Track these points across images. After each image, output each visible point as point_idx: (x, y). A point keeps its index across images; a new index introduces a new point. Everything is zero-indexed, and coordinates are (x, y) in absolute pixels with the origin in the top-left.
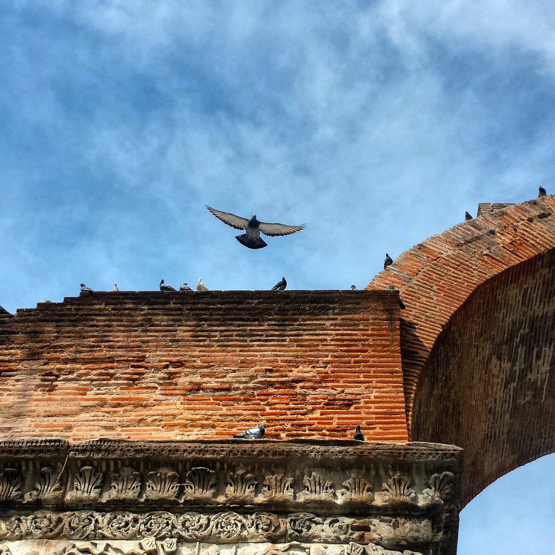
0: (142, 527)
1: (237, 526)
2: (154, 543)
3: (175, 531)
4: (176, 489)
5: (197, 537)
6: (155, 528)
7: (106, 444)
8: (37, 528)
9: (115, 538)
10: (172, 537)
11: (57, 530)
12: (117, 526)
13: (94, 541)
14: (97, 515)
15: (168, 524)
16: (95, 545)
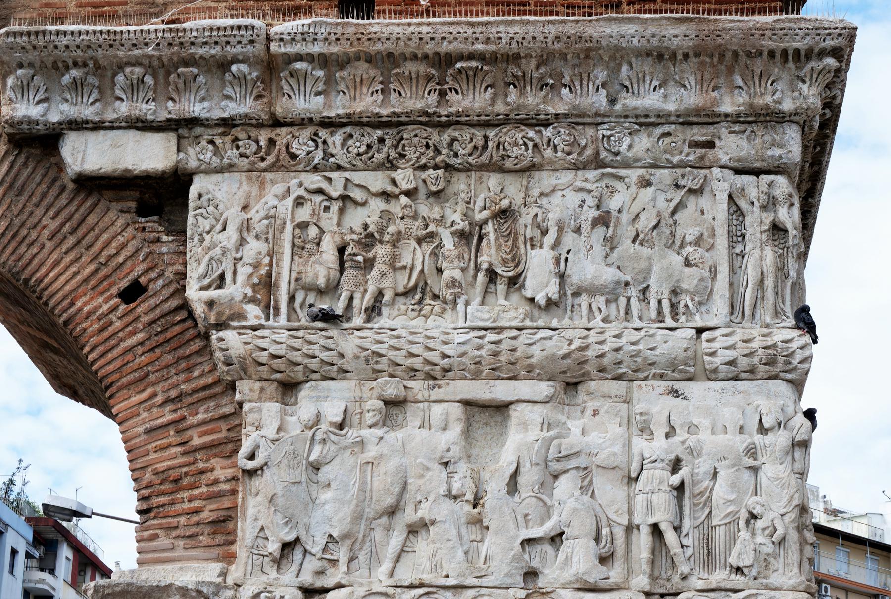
0: (393, 153)
1: (527, 149)
2: (412, 178)
3: (439, 159)
4: (434, 97)
5: (471, 165)
6: (411, 154)
7: (323, 30)
8: (241, 155)
9: (354, 168)
10: (436, 167)
11: (270, 159)
12: (355, 151)
13: (326, 174)
14: (323, 133)
15: (427, 146)
16: (330, 180)
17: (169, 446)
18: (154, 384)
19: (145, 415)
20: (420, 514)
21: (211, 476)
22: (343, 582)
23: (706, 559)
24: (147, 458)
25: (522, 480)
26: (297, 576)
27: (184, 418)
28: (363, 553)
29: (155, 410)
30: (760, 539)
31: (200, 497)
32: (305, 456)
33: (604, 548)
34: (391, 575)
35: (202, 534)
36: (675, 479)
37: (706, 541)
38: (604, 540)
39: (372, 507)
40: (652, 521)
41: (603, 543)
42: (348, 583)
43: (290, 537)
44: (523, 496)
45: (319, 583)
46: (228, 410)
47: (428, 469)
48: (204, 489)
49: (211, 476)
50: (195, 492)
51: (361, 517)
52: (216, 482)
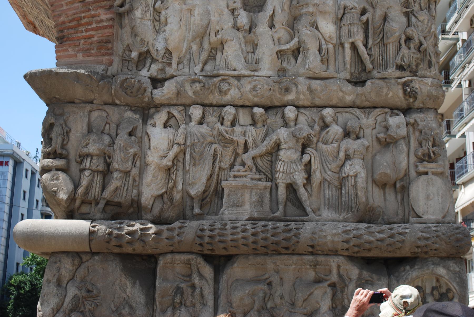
21: (98, 18)
22: (175, 74)
23: (381, 62)
25: (276, 19)
26: (148, 71)
30: (413, 50)
31: (92, 29)
32: (152, 5)
33: (324, 56)
34: (202, 70)
35: (93, 49)
36: (364, 18)
37: (381, 52)
38: (323, 51)
39: (191, 33)
40: (351, 40)
41: (323, 53)
42: (177, 75)
43: (144, 49)
48: (94, 25)
49: (98, 18)
50: (90, 27)
52: (102, 21)
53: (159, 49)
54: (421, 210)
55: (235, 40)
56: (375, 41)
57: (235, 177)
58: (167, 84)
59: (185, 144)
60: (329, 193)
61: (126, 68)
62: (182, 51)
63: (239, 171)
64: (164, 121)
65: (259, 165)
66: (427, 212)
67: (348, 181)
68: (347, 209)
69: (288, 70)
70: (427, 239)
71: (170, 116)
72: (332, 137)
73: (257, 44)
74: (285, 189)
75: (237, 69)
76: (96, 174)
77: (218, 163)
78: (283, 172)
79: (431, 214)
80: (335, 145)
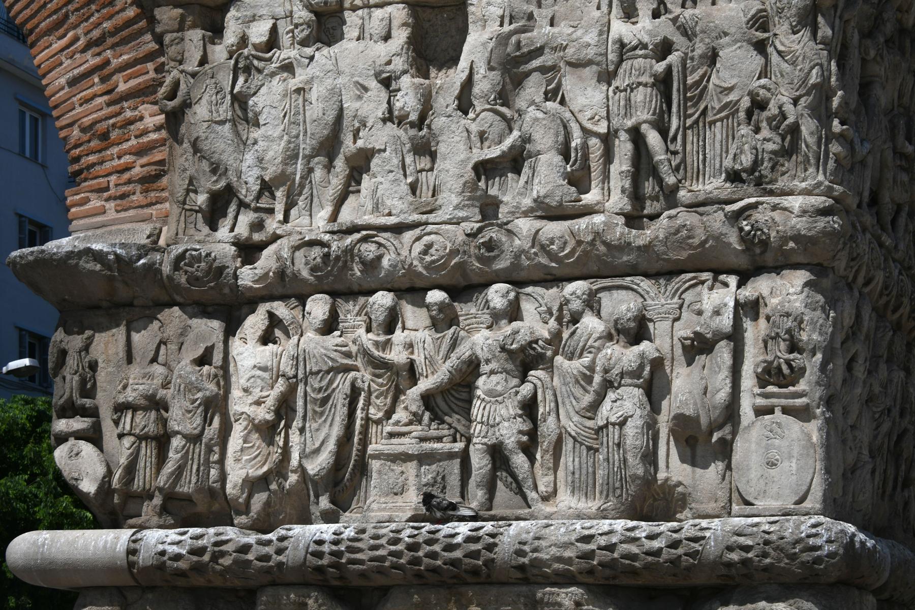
17: (95, 96)
18: (75, 27)
19: (67, 63)
20: (360, 143)
24: (74, 112)
26: (232, 230)
27: (107, 62)
28: (302, 198)
29: (78, 56)
34: (334, 217)
38: (573, 155)
39: (308, 142)
44: (478, 109)
45: (257, 237)
46: (153, 46)
47: (366, 89)
48: (133, 142)
49: (140, 126)
51: (296, 156)
53: (251, 180)
54: (753, 489)
55: (388, 149)
56: (687, 117)
57: (392, 435)
58: (265, 252)
59: (296, 376)
60: (574, 461)
61: (193, 226)
62: (294, 180)
63: (397, 423)
64: (260, 333)
65: (441, 411)
66: (765, 492)
67: (608, 435)
68: (605, 493)
69: (501, 202)
70: (746, 549)
71: (274, 321)
72: (581, 344)
73: (436, 151)
74: (488, 457)
75: (394, 212)
76: (144, 444)
77: (363, 409)
78: (482, 423)
79: (772, 497)
80: (586, 360)
